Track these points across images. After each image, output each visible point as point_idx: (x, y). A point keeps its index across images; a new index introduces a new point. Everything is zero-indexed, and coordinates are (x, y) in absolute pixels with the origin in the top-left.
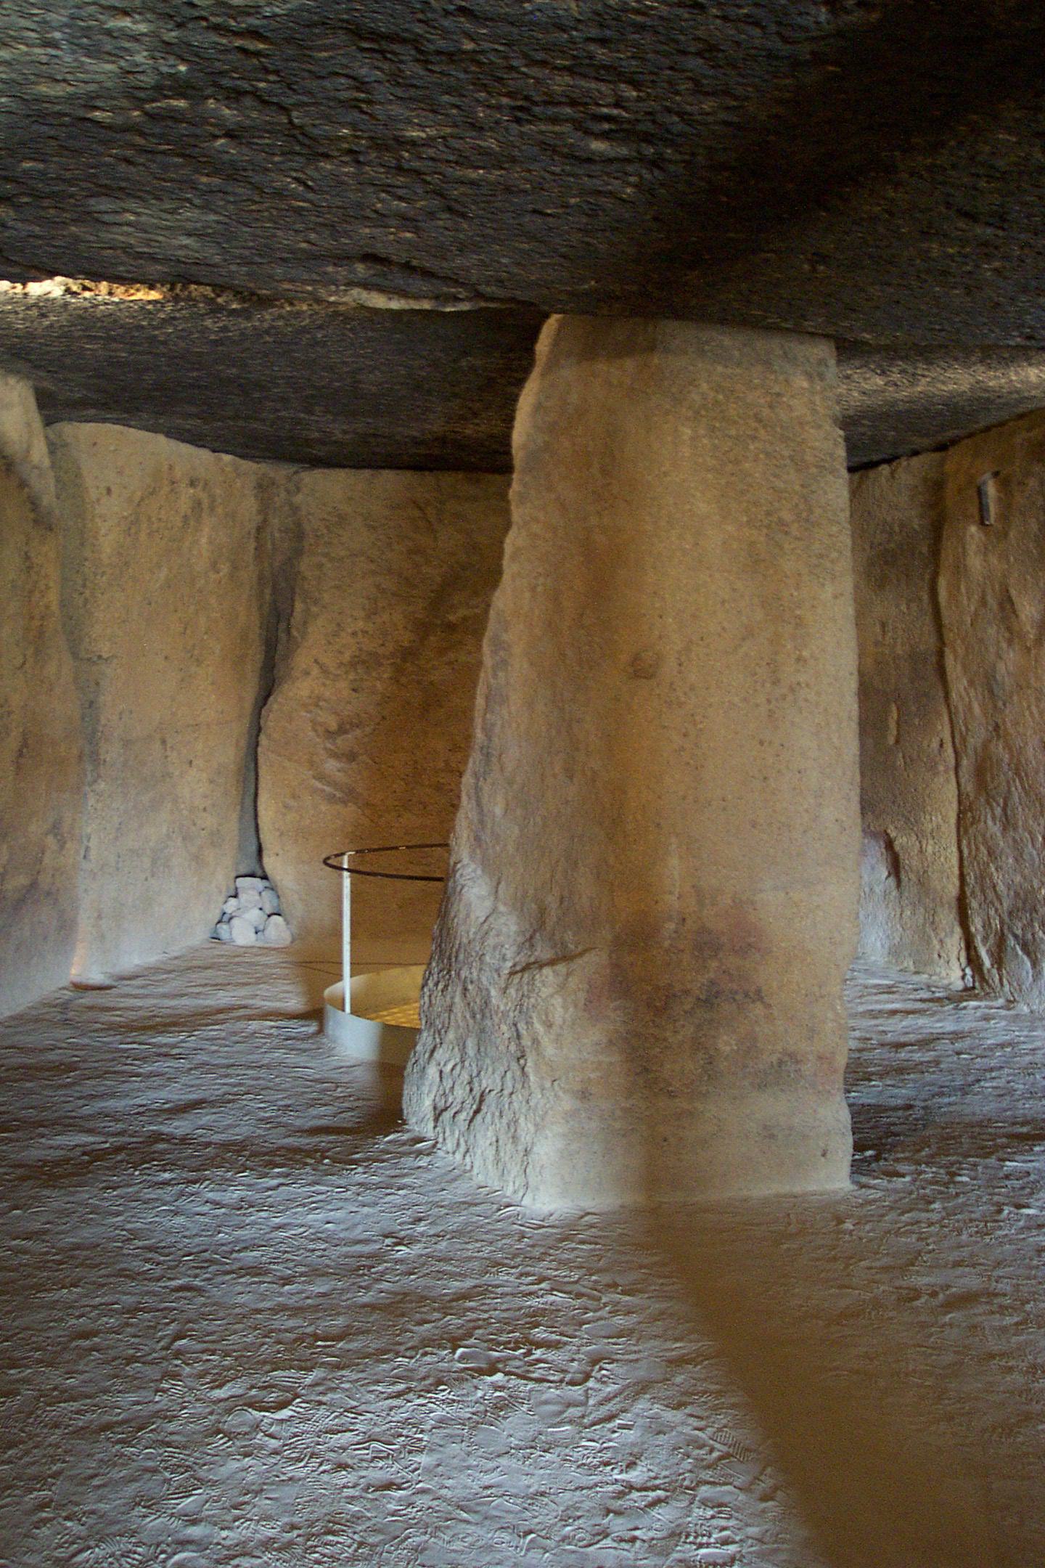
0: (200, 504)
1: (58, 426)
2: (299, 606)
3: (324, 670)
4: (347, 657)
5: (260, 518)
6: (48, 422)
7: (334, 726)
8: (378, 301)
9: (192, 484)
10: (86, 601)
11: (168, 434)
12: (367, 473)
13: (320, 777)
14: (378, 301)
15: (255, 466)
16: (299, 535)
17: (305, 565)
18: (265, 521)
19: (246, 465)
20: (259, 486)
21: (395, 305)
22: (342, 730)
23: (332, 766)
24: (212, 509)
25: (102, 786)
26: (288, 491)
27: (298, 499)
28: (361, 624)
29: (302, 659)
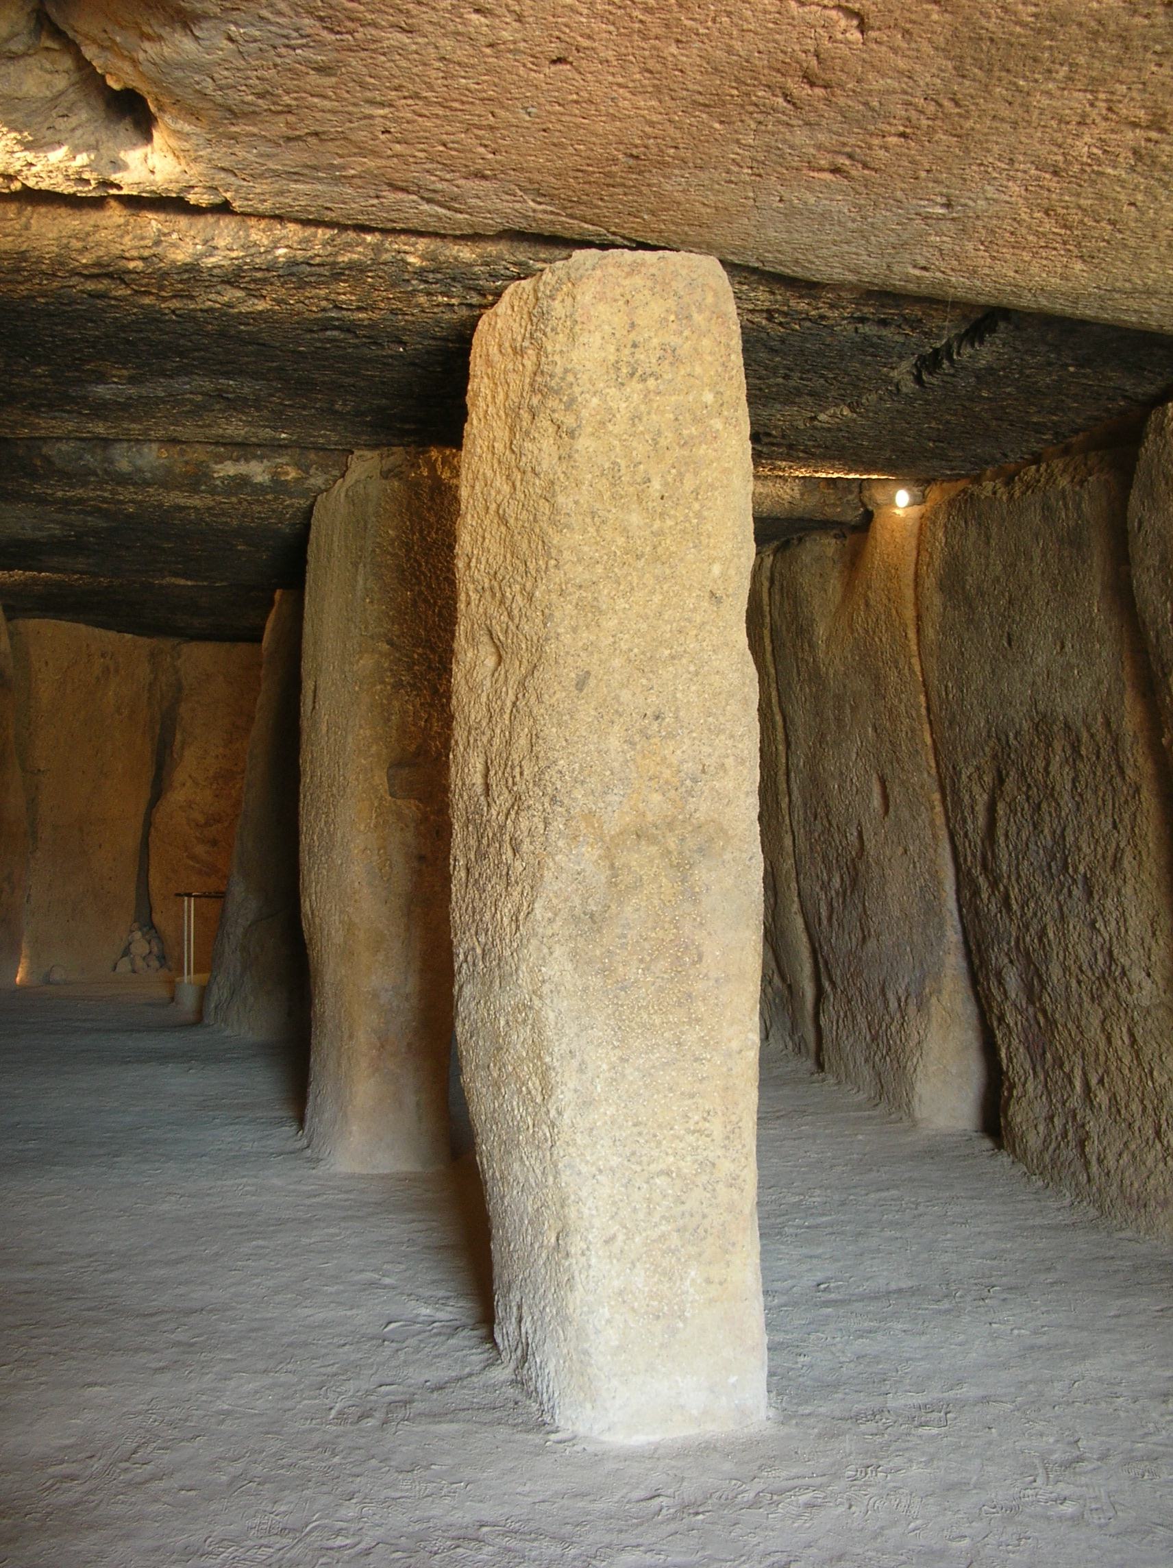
0: (108, 669)
1: (15, 621)
2: (179, 737)
3: (196, 784)
4: (211, 773)
5: (152, 676)
6: (9, 619)
7: (202, 820)
8: (182, 582)
9: (103, 655)
10: (31, 734)
11: (87, 623)
12: (227, 645)
13: (193, 857)
14: (182, 582)
15: (149, 641)
16: (180, 689)
17: (183, 709)
18: (155, 678)
19: (143, 641)
20: (152, 655)
21: (189, 583)
22: (207, 824)
23: (200, 850)
24: (117, 671)
25: (38, 854)
26: (172, 657)
27: (178, 663)
28: (221, 750)
29: (180, 775)
